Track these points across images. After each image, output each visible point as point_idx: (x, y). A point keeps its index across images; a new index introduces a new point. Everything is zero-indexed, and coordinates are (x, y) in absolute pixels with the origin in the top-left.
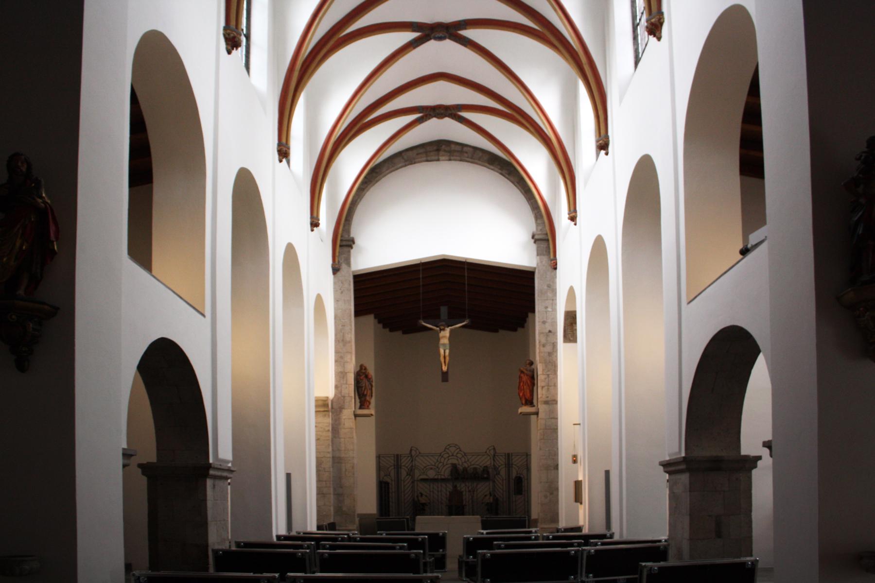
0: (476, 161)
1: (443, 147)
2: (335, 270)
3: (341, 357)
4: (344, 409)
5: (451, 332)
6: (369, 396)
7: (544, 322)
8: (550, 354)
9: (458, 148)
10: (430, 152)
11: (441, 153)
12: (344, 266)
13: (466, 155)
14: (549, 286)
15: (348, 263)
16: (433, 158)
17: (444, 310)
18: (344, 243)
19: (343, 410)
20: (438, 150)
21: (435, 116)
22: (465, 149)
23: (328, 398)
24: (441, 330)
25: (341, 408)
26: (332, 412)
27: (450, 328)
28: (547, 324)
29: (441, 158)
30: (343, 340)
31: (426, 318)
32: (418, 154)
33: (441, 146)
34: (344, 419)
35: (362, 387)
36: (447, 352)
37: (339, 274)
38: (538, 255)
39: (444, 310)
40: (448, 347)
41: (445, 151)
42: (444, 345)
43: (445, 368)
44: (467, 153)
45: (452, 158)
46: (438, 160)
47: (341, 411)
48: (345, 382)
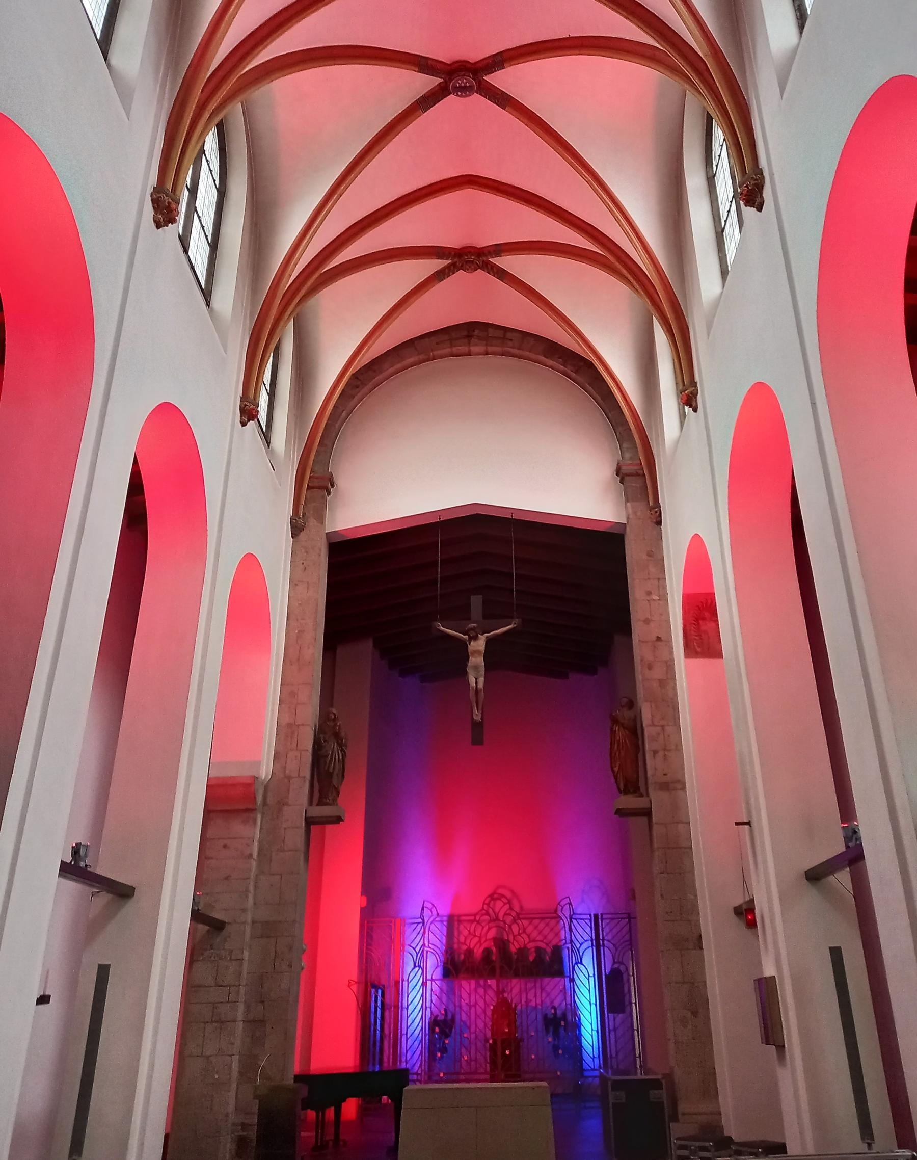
0: (527, 353)
1: (476, 332)
2: (297, 529)
3: (293, 694)
4: (287, 804)
5: (489, 642)
6: (337, 775)
7: (647, 621)
8: (662, 683)
9: (499, 333)
10: (457, 339)
11: (473, 340)
12: (312, 522)
13: (510, 344)
14: (650, 554)
15: (321, 519)
16: (464, 349)
17: (476, 602)
18: (316, 483)
19: (285, 808)
20: (469, 337)
21: (461, 268)
22: (509, 335)
23: (255, 778)
24: (471, 639)
25: (282, 803)
26: (263, 814)
27: (486, 634)
28: (652, 624)
29: (474, 349)
30: (298, 660)
31: (445, 618)
32: (437, 343)
33: (474, 331)
34: (285, 829)
35: (327, 756)
36: (481, 680)
37: (302, 535)
38: (627, 501)
39: (476, 602)
40: (483, 672)
41: (479, 338)
42: (476, 668)
43: (477, 716)
44: (511, 340)
45: (490, 349)
46: (469, 354)
47: (280, 811)
48: (294, 744)
